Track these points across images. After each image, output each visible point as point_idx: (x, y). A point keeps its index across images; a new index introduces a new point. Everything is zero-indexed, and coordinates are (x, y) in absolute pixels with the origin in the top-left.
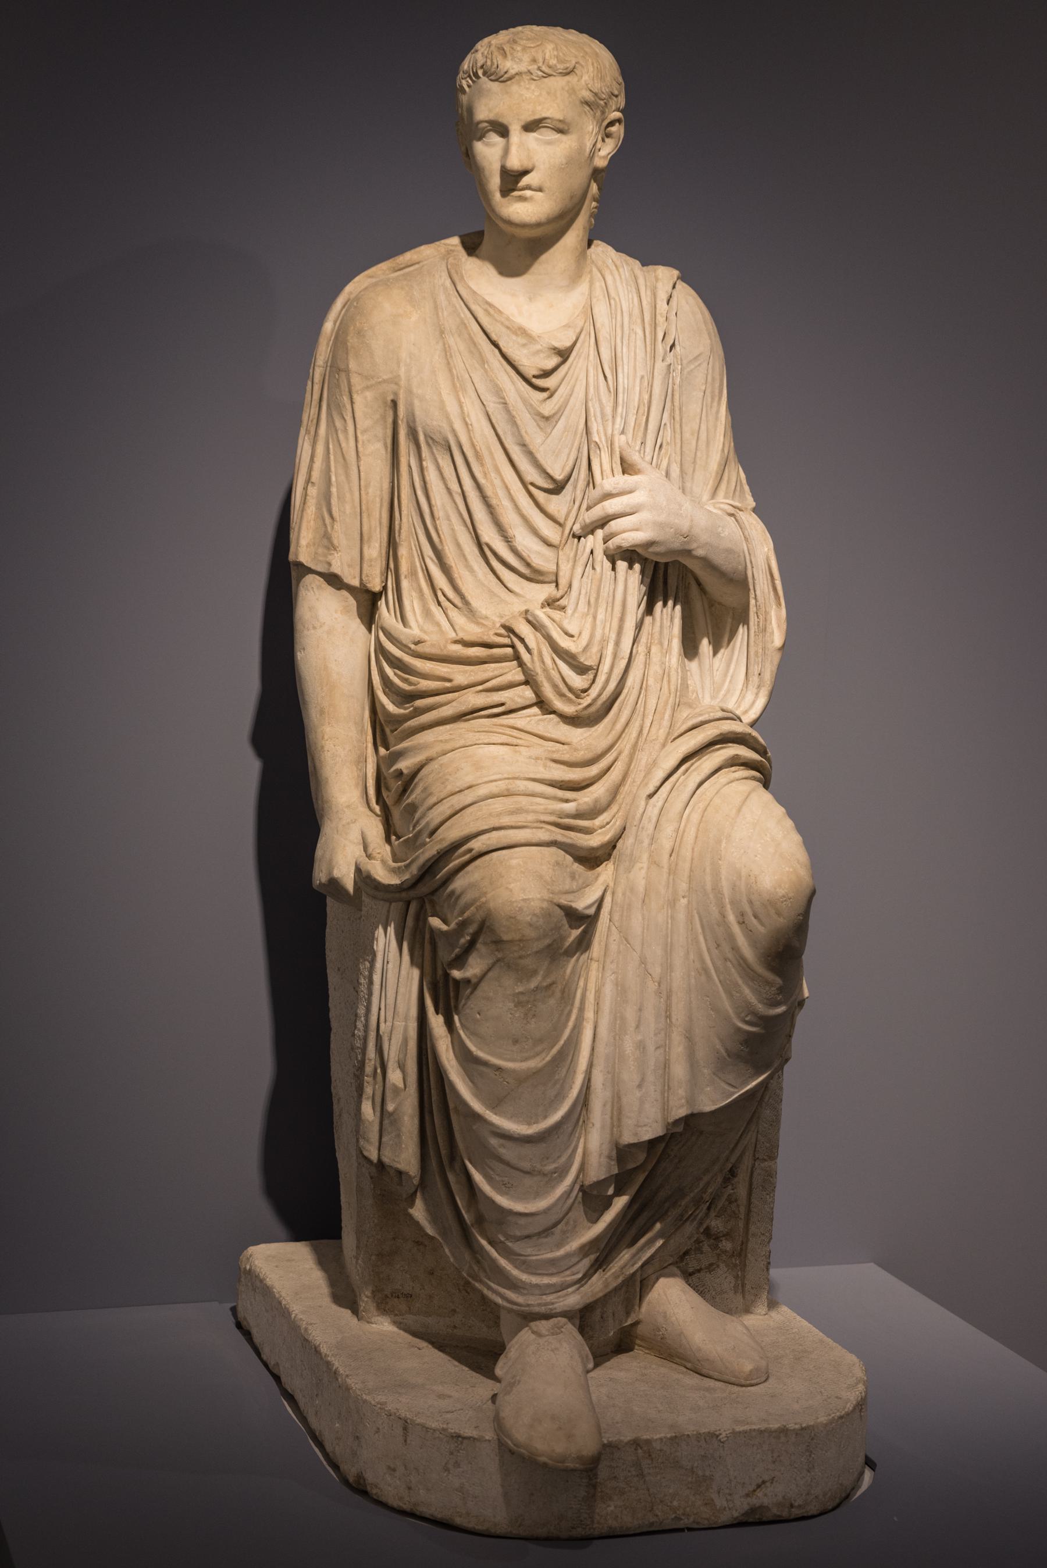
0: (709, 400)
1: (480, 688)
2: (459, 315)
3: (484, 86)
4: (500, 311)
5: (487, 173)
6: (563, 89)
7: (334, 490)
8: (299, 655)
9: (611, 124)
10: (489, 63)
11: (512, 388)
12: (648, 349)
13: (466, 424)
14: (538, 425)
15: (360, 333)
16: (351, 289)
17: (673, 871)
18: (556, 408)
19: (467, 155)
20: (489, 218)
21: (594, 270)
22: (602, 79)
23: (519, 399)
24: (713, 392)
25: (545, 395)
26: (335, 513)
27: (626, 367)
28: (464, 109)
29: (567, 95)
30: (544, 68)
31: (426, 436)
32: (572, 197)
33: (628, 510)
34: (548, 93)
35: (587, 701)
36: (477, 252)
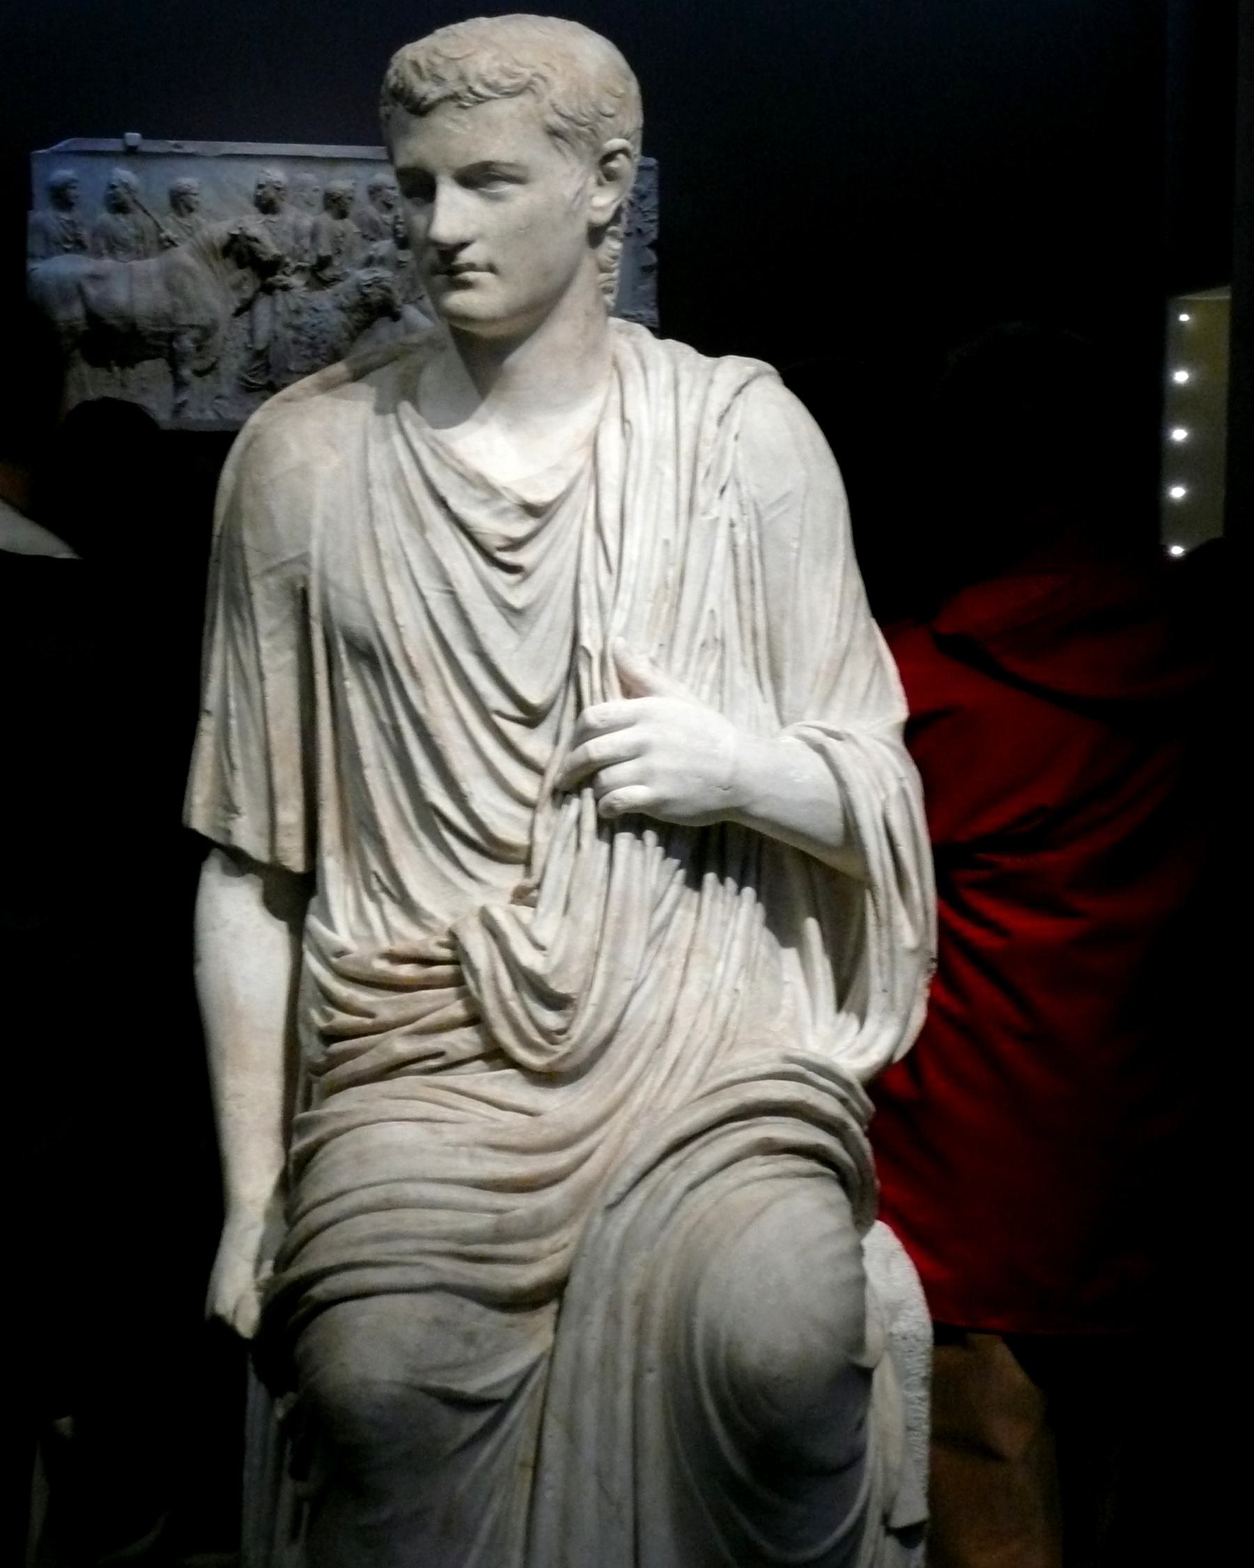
1: (408, 1028)
7: (233, 722)
8: (199, 970)
15: (257, 491)
17: (641, 1328)
26: (237, 760)
32: (547, 274)
33: (623, 753)
35: (562, 1050)
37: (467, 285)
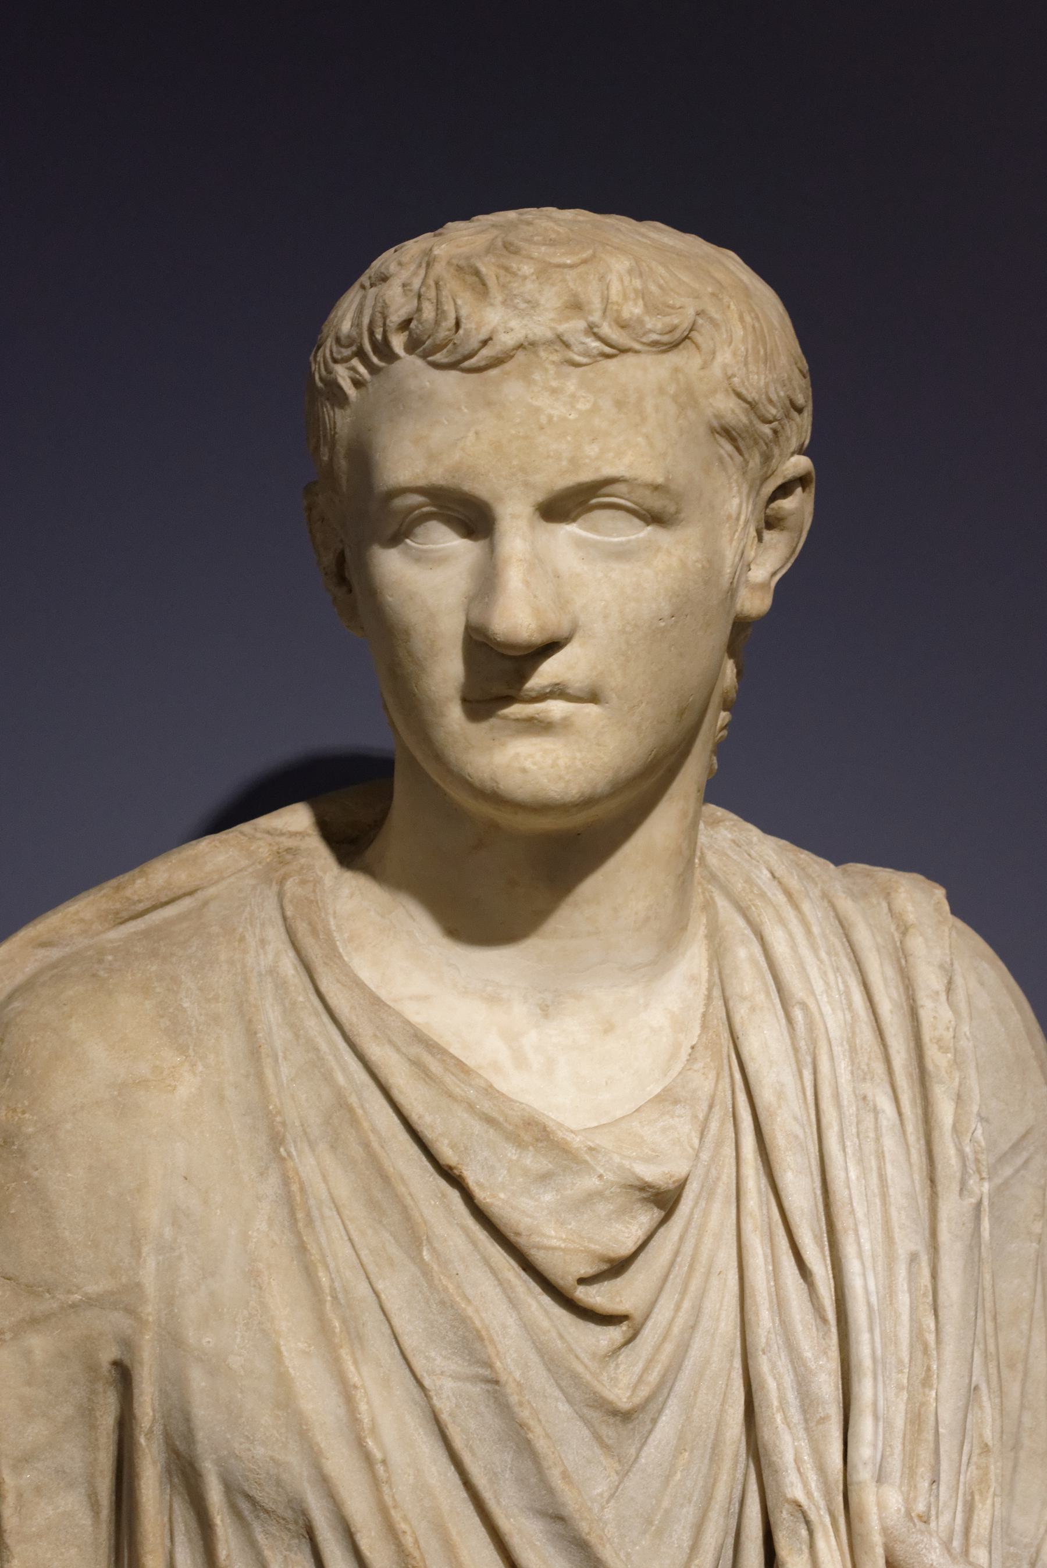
2: (328, 1077)
3: (412, 384)
4: (460, 1064)
5: (419, 645)
6: (661, 391)
10: (428, 312)
11: (511, 1321)
13: (367, 1458)
14: (598, 1438)
18: (654, 1377)
19: (342, 578)
21: (722, 903)
22: (767, 360)
23: (534, 1358)
25: (615, 1334)
27: (864, 1233)
28: (341, 450)
30: (606, 329)
31: (229, 1489)
32: (681, 712)
34: (619, 404)
36: (370, 854)
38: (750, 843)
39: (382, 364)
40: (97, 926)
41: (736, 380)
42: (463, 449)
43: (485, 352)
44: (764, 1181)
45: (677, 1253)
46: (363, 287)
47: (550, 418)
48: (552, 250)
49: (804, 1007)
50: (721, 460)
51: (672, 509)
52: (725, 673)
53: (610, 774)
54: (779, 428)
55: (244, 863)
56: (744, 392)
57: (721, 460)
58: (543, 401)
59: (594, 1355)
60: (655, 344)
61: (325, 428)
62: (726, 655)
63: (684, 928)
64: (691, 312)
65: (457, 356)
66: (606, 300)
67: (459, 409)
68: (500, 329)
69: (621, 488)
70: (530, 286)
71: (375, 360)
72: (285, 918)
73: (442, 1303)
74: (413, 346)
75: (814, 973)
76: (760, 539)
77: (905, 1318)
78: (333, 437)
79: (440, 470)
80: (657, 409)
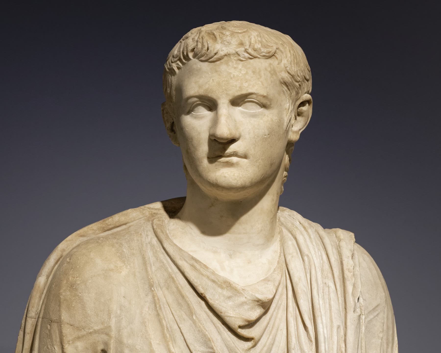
0: (385, 346)
2: (166, 270)
3: (195, 66)
4: (205, 266)
5: (195, 142)
6: (266, 69)
9: (303, 104)
10: (200, 46)
11: (219, 338)
12: (340, 301)
15: (72, 287)
16: (65, 246)
19: (172, 130)
20: (193, 183)
21: (284, 230)
22: (297, 64)
24: (387, 339)
25: (250, 344)
27: (324, 318)
28: (173, 88)
29: (269, 75)
30: (250, 51)
32: (271, 165)
34: (254, 72)
36: (179, 214)
37: (230, 164)
38: (294, 215)
39: (186, 62)
40: (97, 232)
41: (288, 68)
42: (209, 84)
43: (216, 57)
44: (295, 304)
45: (268, 323)
46: (181, 42)
47: (234, 75)
48: (235, 28)
49: (308, 256)
50: (283, 92)
51: (269, 104)
52: (285, 159)
53: (250, 180)
54: (301, 84)
55: (141, 216)
56: (290, 72)
57: (283, 92)
58: (232, 71)
59: (243, 350)
60: (264, 56)
61: (169, 83)
62: (285, 153)
63: (273, 237)
64: (275, 48)
65: (208, 58)
66: (250, 43)
67: (208, 73)
68: (220, 50)
69: (254, 96)
70: (229, 38)
71: (184, 61)
72: (153, 229)
73: (199, 331)
74: (195, 56)
75: (311, 249)
76: (296, 119)
77: (336, 342)
78: (171, 85)
79: (202, 90)
80: (265, 74)
